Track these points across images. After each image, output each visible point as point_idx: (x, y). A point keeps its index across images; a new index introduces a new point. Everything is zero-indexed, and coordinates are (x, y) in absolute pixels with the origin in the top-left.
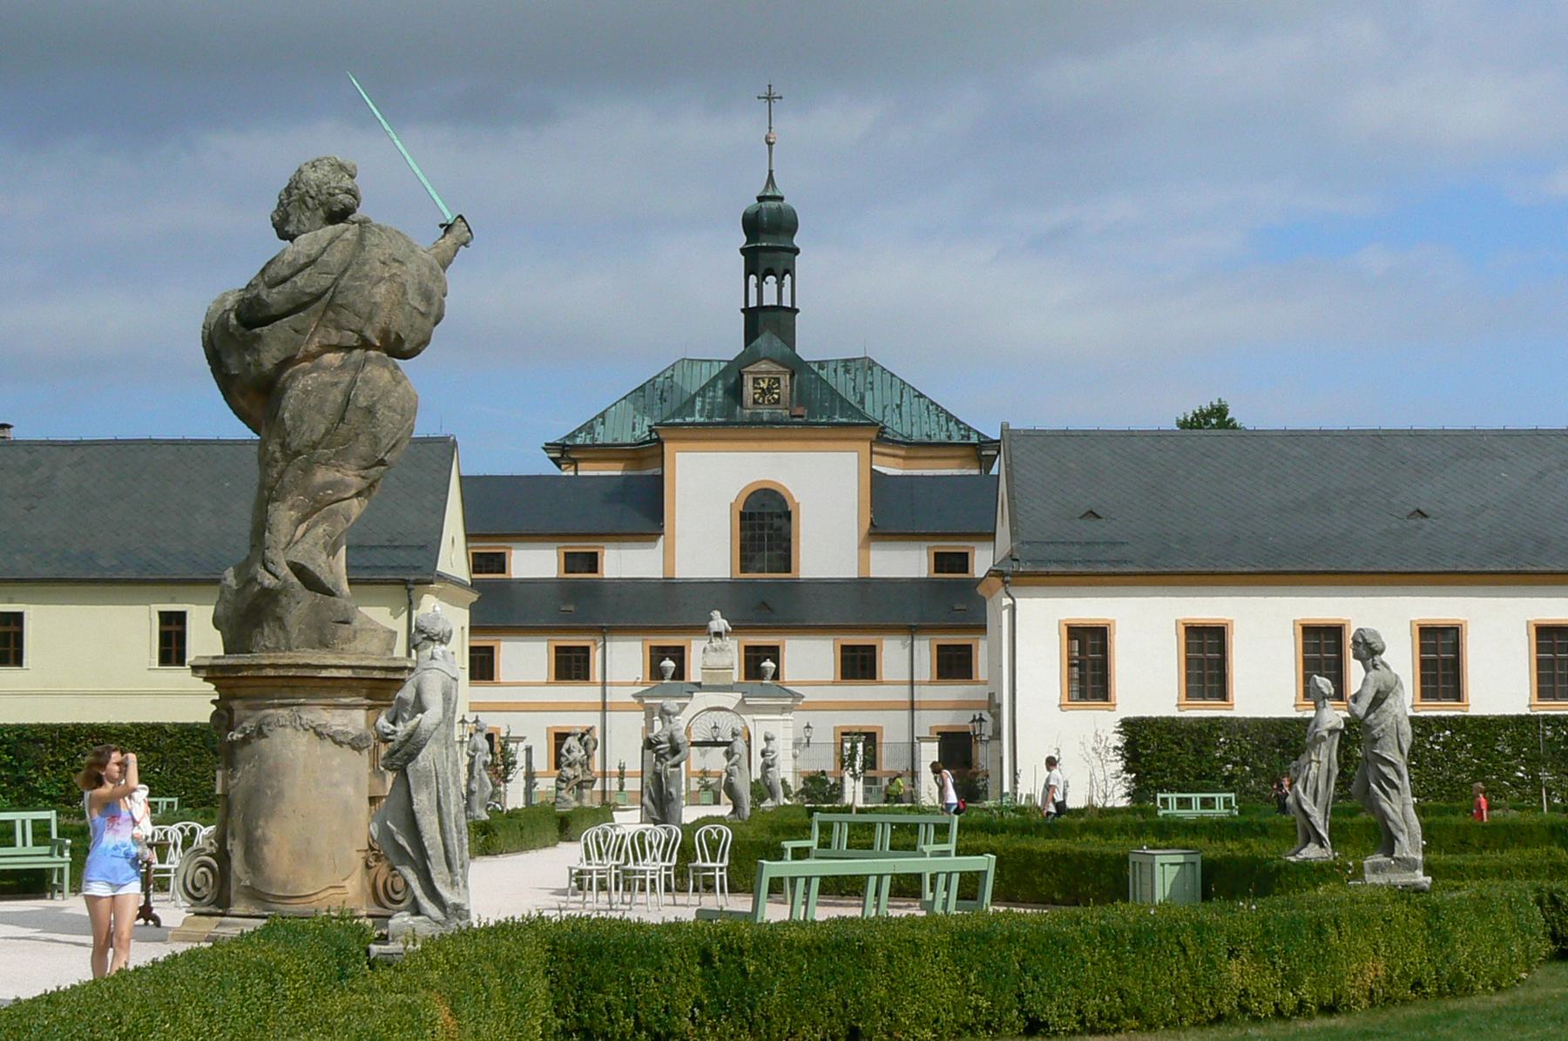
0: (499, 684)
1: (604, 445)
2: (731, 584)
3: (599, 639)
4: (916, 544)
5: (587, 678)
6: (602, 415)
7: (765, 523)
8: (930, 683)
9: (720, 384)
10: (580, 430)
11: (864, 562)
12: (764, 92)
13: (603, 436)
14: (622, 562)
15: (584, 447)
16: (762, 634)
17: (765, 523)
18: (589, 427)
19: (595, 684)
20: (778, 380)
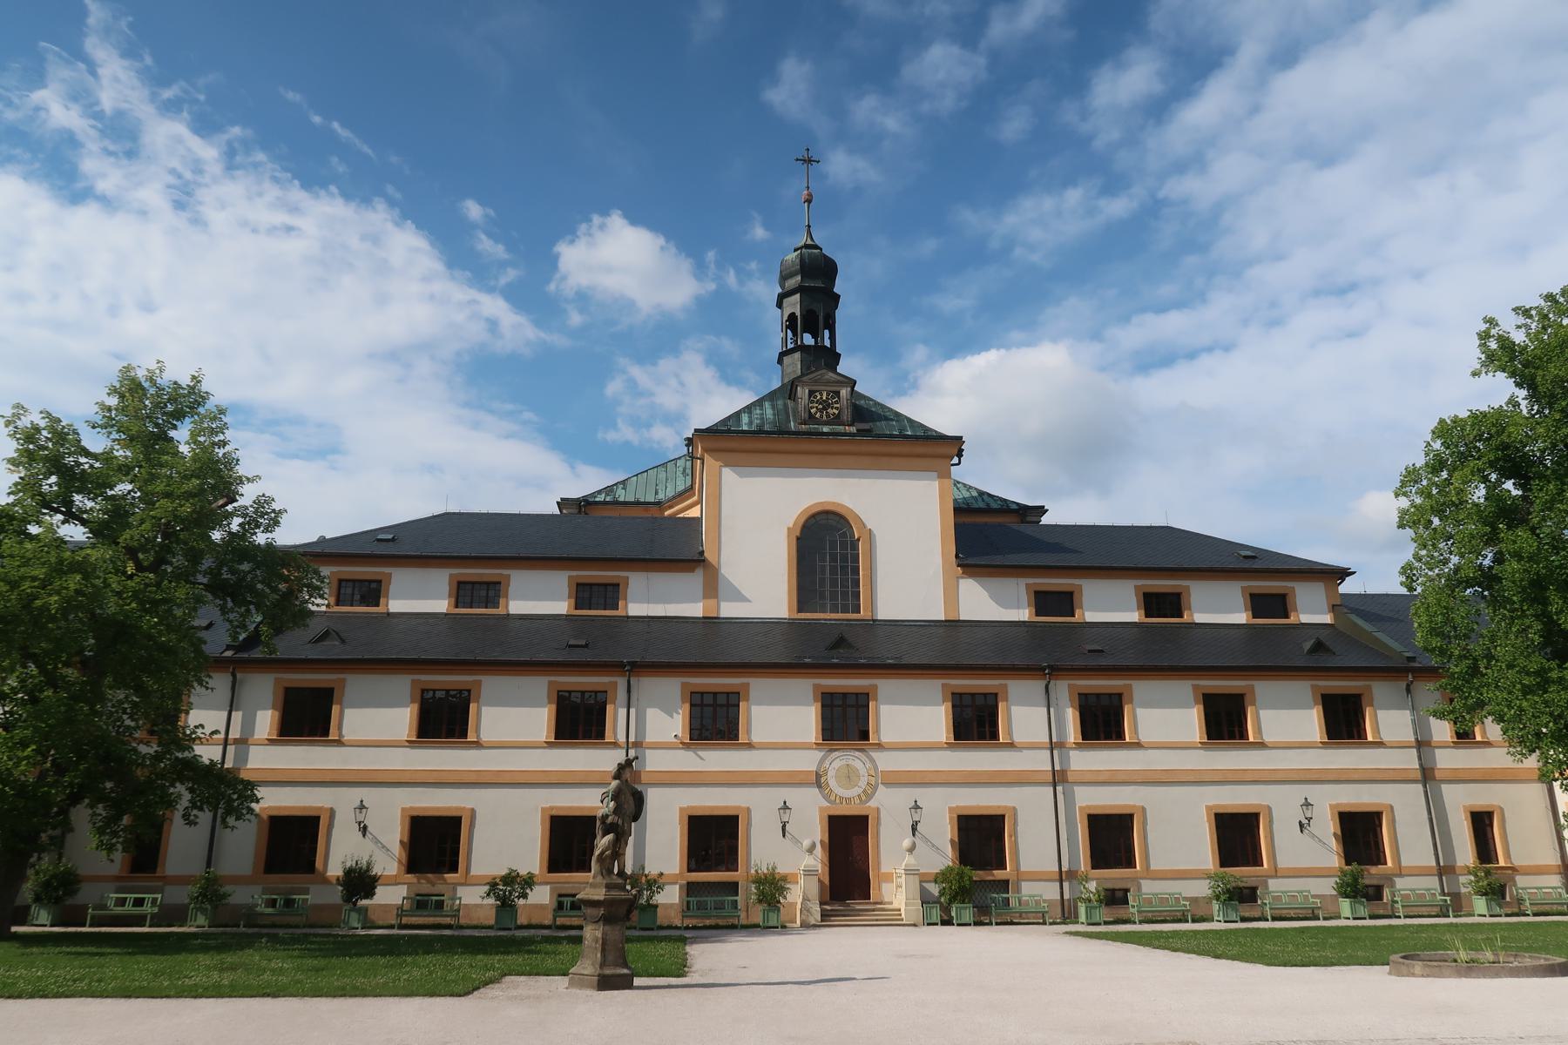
0: (478, 745)
1: (625, 503)
2: (790, 624)
3: (621, 682)
4: (1018, 576)
5: (601, 735)
6: (623, 482)
7: (827, 550)
8: (1078, 746)
9: (767, 405)
10: (599, 492)
11: (951, 596)
12: (802, 154)
13: (621, 495)
14: (651, 599)
15: (605, 503)
16: (846, 676)
17: (827, 550)
18: (609, 490)
19: (615, 745)
20: (837, 393)
